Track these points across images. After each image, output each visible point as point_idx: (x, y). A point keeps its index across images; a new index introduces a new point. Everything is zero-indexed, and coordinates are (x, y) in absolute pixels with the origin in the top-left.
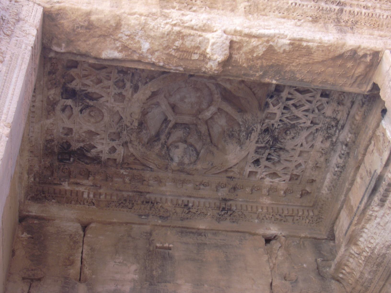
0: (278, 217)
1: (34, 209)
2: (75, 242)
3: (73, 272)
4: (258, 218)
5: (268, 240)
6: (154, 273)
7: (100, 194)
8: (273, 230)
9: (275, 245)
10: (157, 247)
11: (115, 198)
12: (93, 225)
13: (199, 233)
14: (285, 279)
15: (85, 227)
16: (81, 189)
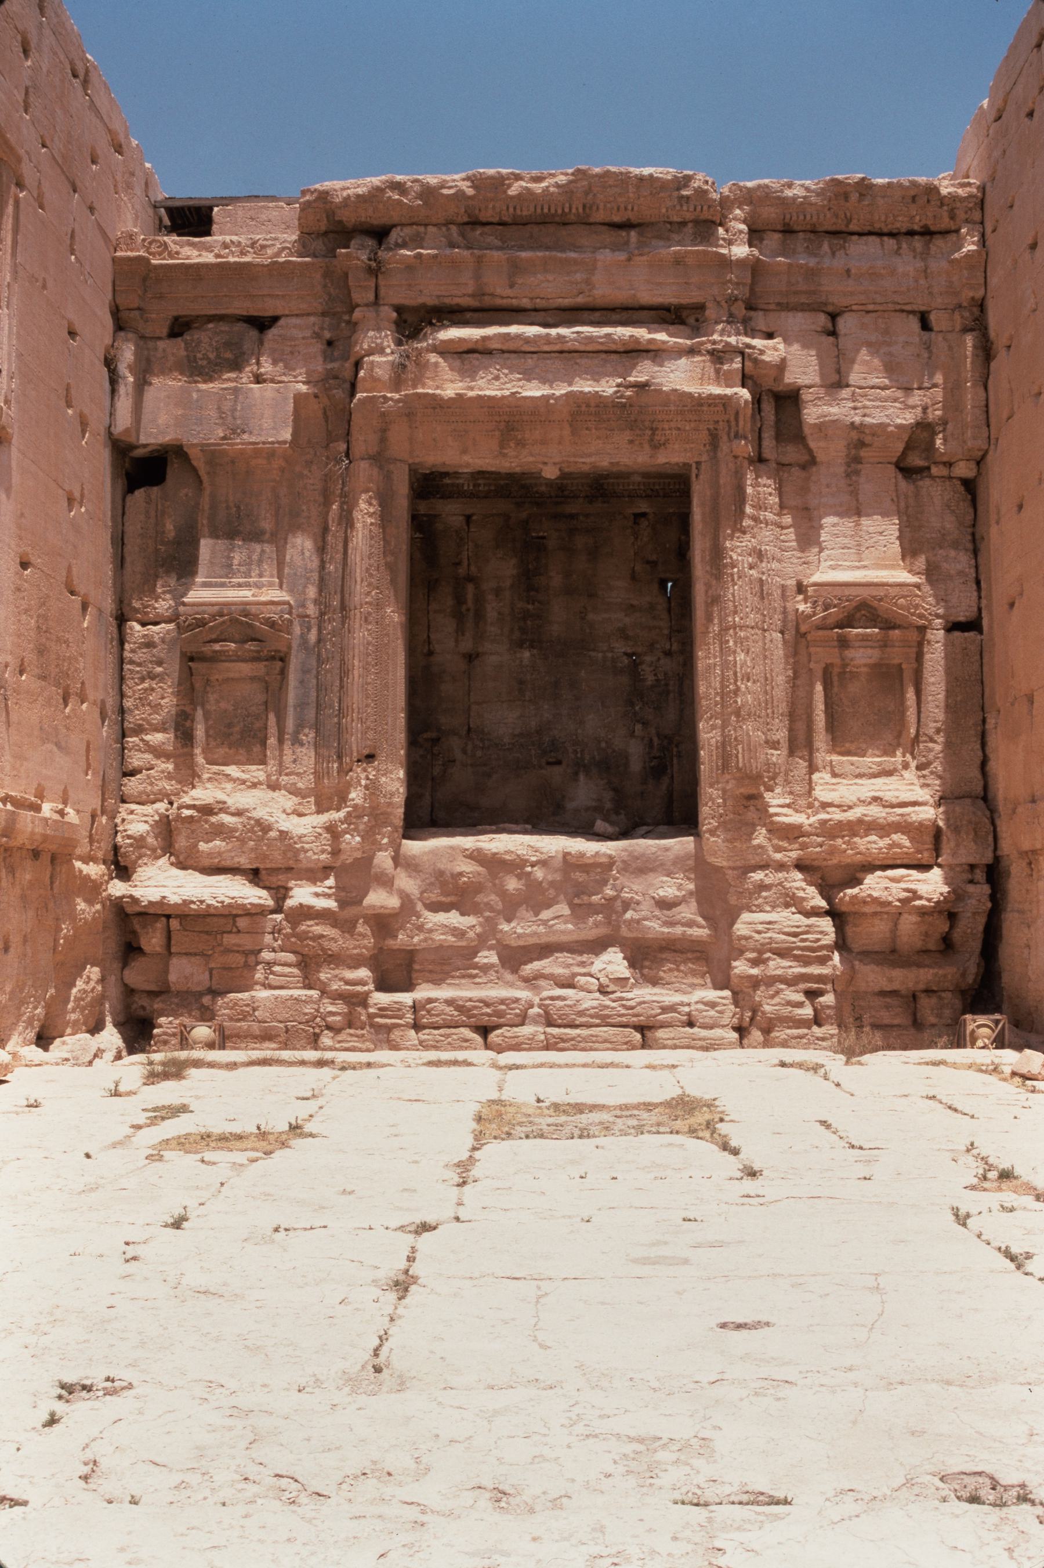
0: (649, 492)
1: (423, 508)
2: (462, 539)
3: (462, 571)
4: (629, 496)
5: (639, 516)
6: (530, 566)
7: (479, 485)
8: (643, 507)
9: (644, 523)
10: (533, 537)
11: (493, 488)
12: (474, 518)
13: (572, 516)
14: (648, 562)
15: (468, 518)
16: (461, 481)
